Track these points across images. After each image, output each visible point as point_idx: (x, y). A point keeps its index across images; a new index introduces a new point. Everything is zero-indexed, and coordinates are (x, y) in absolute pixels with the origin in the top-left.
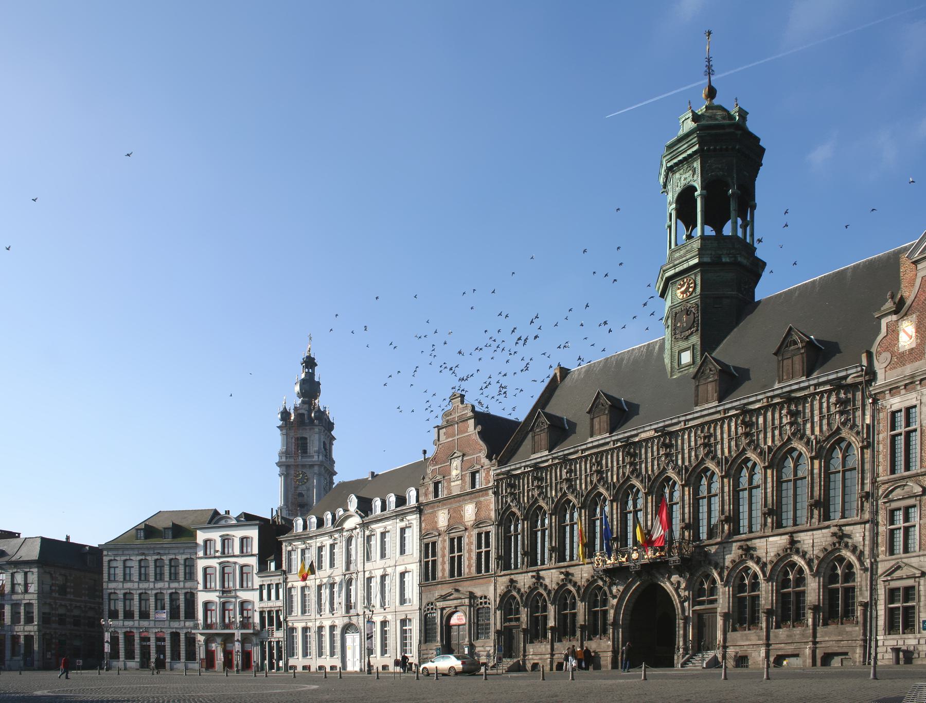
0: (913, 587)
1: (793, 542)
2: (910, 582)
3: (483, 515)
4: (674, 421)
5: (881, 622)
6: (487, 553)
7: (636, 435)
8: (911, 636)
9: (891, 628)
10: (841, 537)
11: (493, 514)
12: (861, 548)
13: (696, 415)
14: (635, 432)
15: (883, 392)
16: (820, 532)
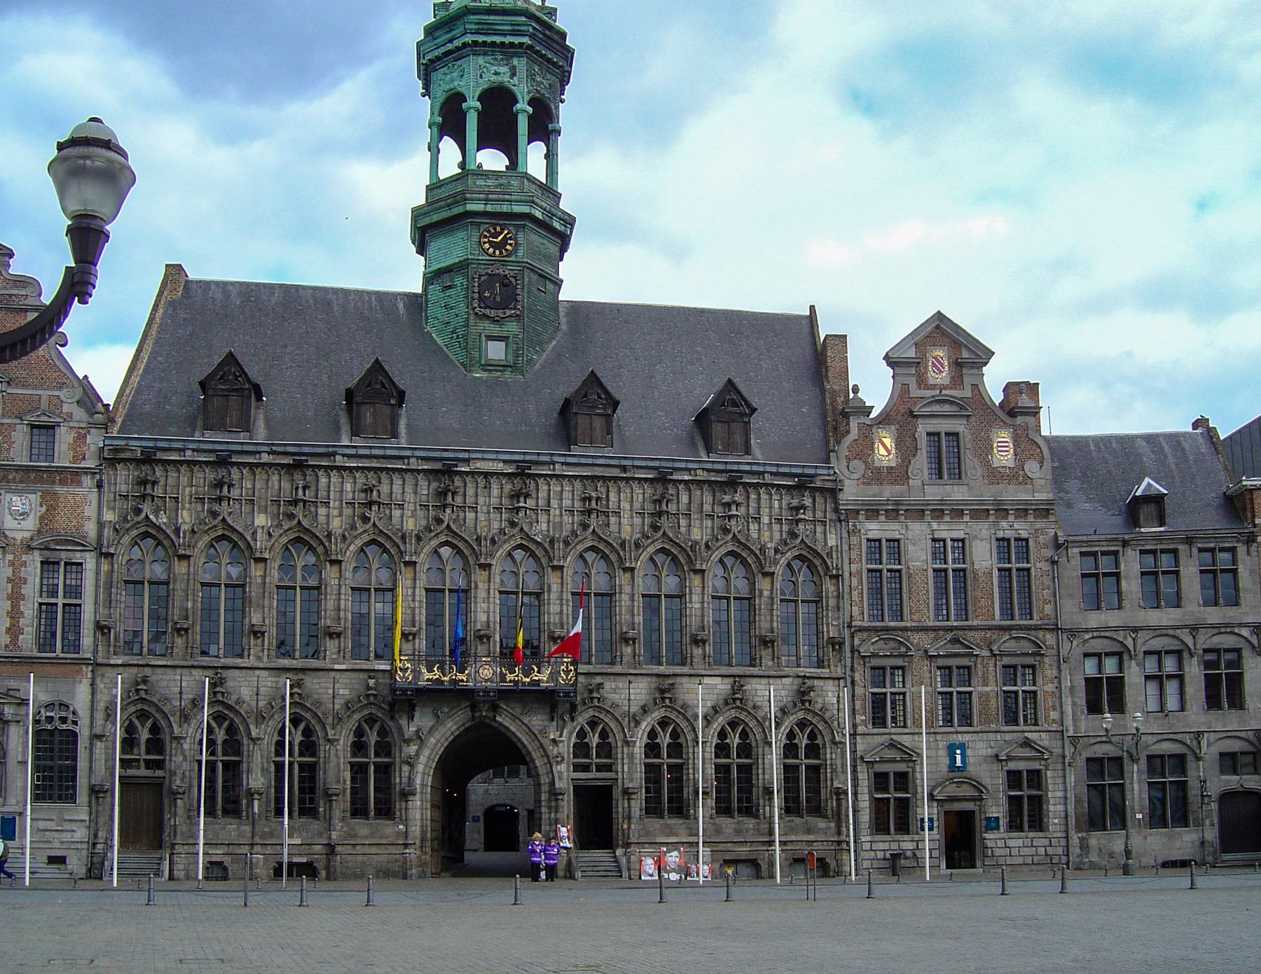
0: (906, 774)
1: (737, 688)
2: (902, 767)
3: (63, 523)
4: (542, 458)
5: (865, 817)
6: (73, 611)
7: (467, 461)
8: (906, 837)
9: (880, 826)
10: (803, 695)
11: (91, 529)
12: (835, 712)
13: (583, 461)
14: (466, 455)
15: (858, 512)
16: (778, 681)
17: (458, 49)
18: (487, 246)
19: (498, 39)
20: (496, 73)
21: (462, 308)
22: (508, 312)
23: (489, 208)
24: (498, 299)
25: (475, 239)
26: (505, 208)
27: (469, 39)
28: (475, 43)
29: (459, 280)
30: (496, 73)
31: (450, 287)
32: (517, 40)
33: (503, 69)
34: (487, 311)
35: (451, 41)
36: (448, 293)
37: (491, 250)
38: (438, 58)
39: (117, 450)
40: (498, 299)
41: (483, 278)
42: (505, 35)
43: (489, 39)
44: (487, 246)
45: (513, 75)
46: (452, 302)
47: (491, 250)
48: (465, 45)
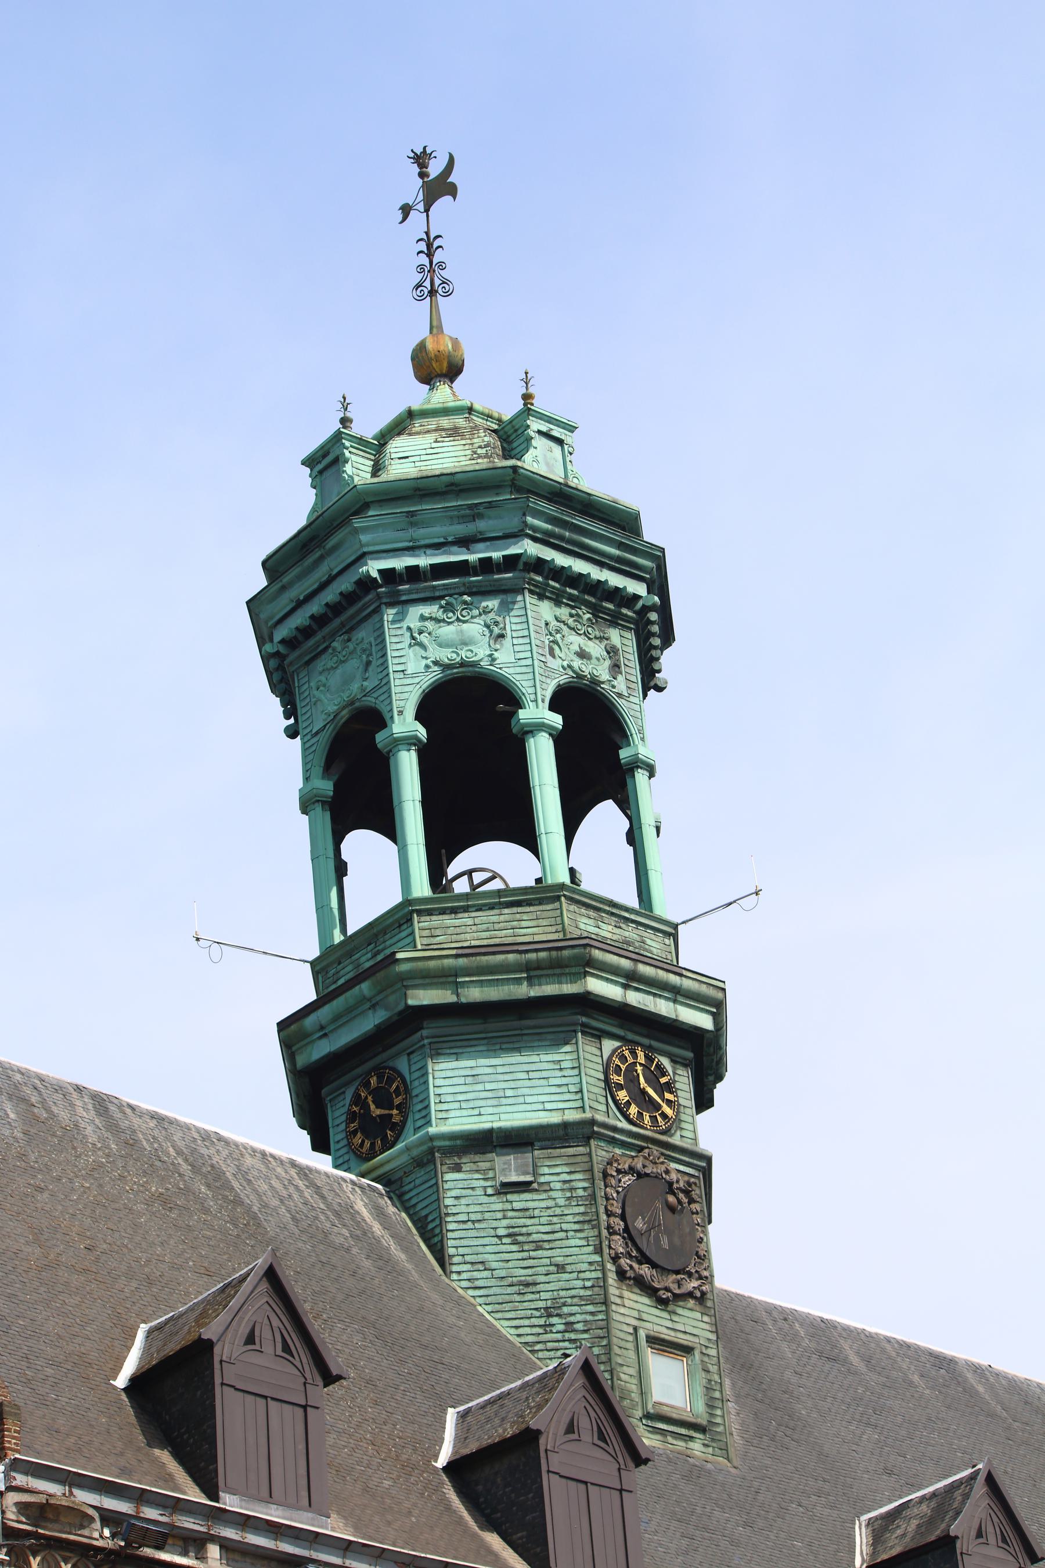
17: (486, 565)
19: (580, 567)
20: (582, 655)
21: (578, 1250)
23: (634, 998)
25: (594, 1072)
26: (663, 1007)
27: (530, 548)
28: (539, 565)
29: (555, 1171)
30: (582, 655)
31: (522, 1187)
32: (615, 580)
33: (596, 649)
34: (645, 1270)
35: (465, 542)
36: (519, 1200)
37: (633, 1110)
38: (413, 574)
39: (41, 1511)
42: (601, 565)
43: (562, 560)
44: (623, 1095)
45: (615, 668)
46: (537, 1230)
48: (511, 562)
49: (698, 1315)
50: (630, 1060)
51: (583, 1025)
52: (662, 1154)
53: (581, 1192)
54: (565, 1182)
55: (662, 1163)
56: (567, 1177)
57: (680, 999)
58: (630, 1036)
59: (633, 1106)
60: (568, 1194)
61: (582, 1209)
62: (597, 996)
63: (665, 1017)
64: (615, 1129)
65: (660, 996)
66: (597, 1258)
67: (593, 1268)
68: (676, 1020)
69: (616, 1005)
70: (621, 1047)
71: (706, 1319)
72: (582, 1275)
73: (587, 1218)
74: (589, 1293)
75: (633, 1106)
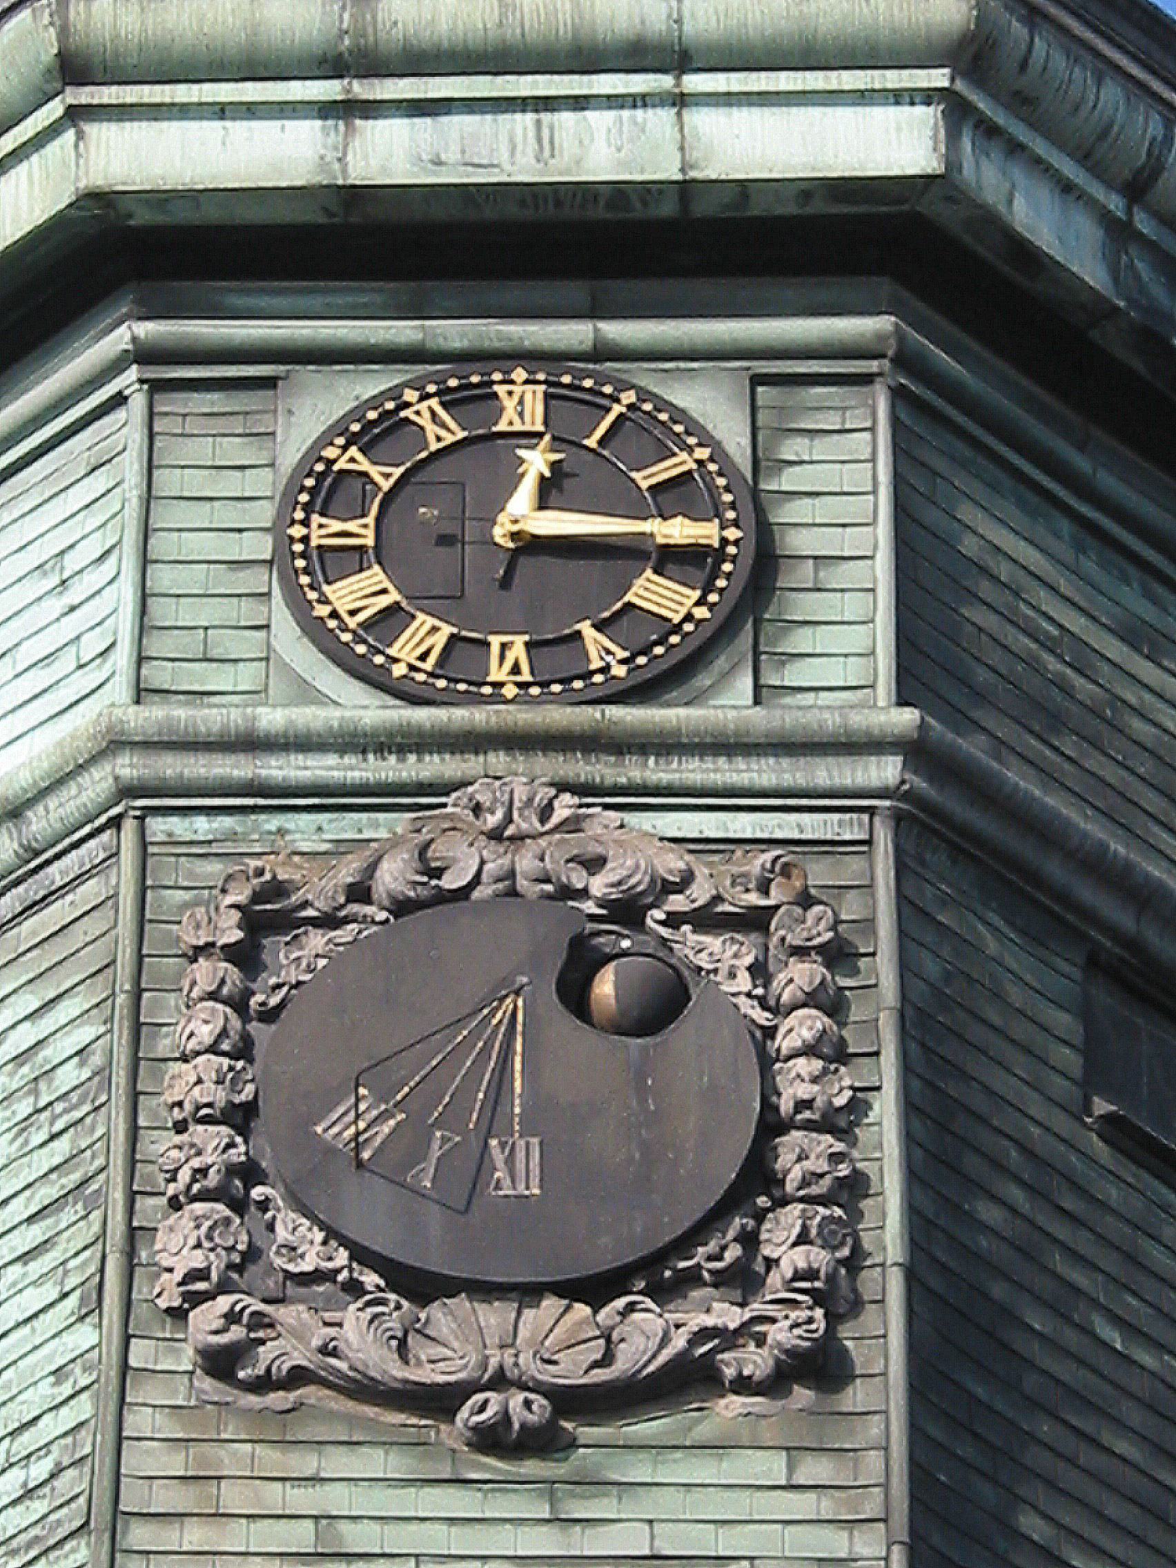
18: (358, 594)
22: (647, 1334)
23: (391, 153)
24: (518, 1172)
26: (606, 145)
40: (518, 1172)
41: (297, 959)
47: (422, 638)
49: (773, 1467)
50: (438, 428)
51: (144, 355)
52: (563, 787)
53: (69, 1076)
54: (20, 1059)
55: (573, 825)
56: (26, 1036)
57: (695, 82)
58: (454, 332)
59: (424, 621)
60: (24, 1108)
61: (62, 1147)
62: (160, 198)
63: (619, 192)
64: (251, 743)
65: (579, 103)
66: (85, 1336)
67: (67, 1389)
68: (686, 188)
69: (310, 215)
70: (394, 393)
71: (815, 1469)
72: (28, 1441)
73: (76, 1177)
74: (39, 1507)
75: (424, 621)
